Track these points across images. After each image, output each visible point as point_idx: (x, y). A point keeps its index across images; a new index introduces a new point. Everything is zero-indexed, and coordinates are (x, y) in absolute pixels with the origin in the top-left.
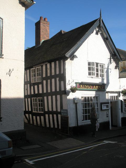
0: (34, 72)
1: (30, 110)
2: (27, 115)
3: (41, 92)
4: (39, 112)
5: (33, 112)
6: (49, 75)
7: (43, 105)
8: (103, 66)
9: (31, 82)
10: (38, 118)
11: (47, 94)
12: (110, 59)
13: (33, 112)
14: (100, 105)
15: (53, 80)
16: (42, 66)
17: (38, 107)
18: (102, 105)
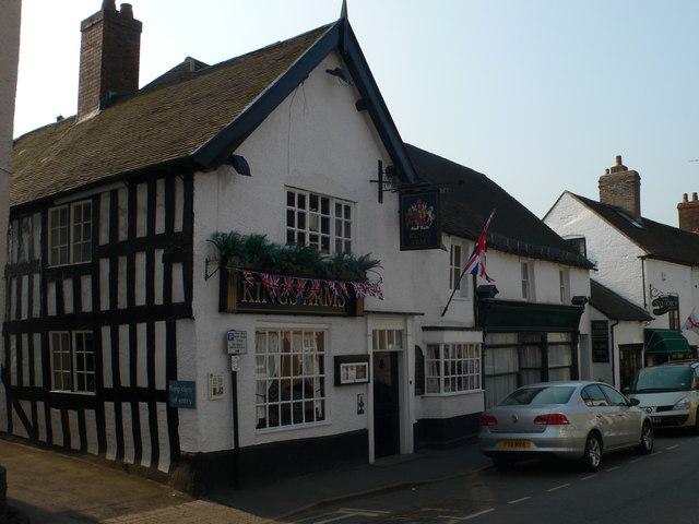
0: (63, 223)
1: (39, 382)
2: (26, 406)
3: (87, 306)
6: (123, 235)
7: (95, 361)
8: (348, 209)
9: (49, 262)
10: (73, 415)
11: (115, 318)
12: (380, 182)
14: (332, 364)
15: (141, 260)
16: (97, 198)
17: (76, 372)
18: (342, 365)
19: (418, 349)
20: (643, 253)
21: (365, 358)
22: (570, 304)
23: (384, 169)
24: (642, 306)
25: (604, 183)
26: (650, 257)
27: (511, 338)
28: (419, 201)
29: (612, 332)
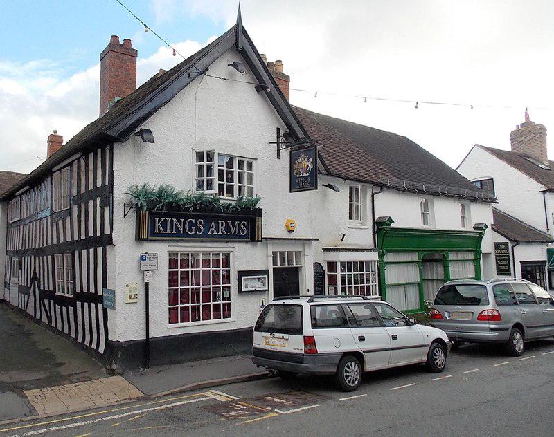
8: (250, 166)
12: (278, 143)
14: (236, 278)
18: (243, 278)
19: (317, 266)
20: (544, 188)
21: (266, 272)
22: (473, 230)
23: (282, 133)
24: (546, 231)
25: (515, 136)
26: (551, 191)
29: (513, 252)
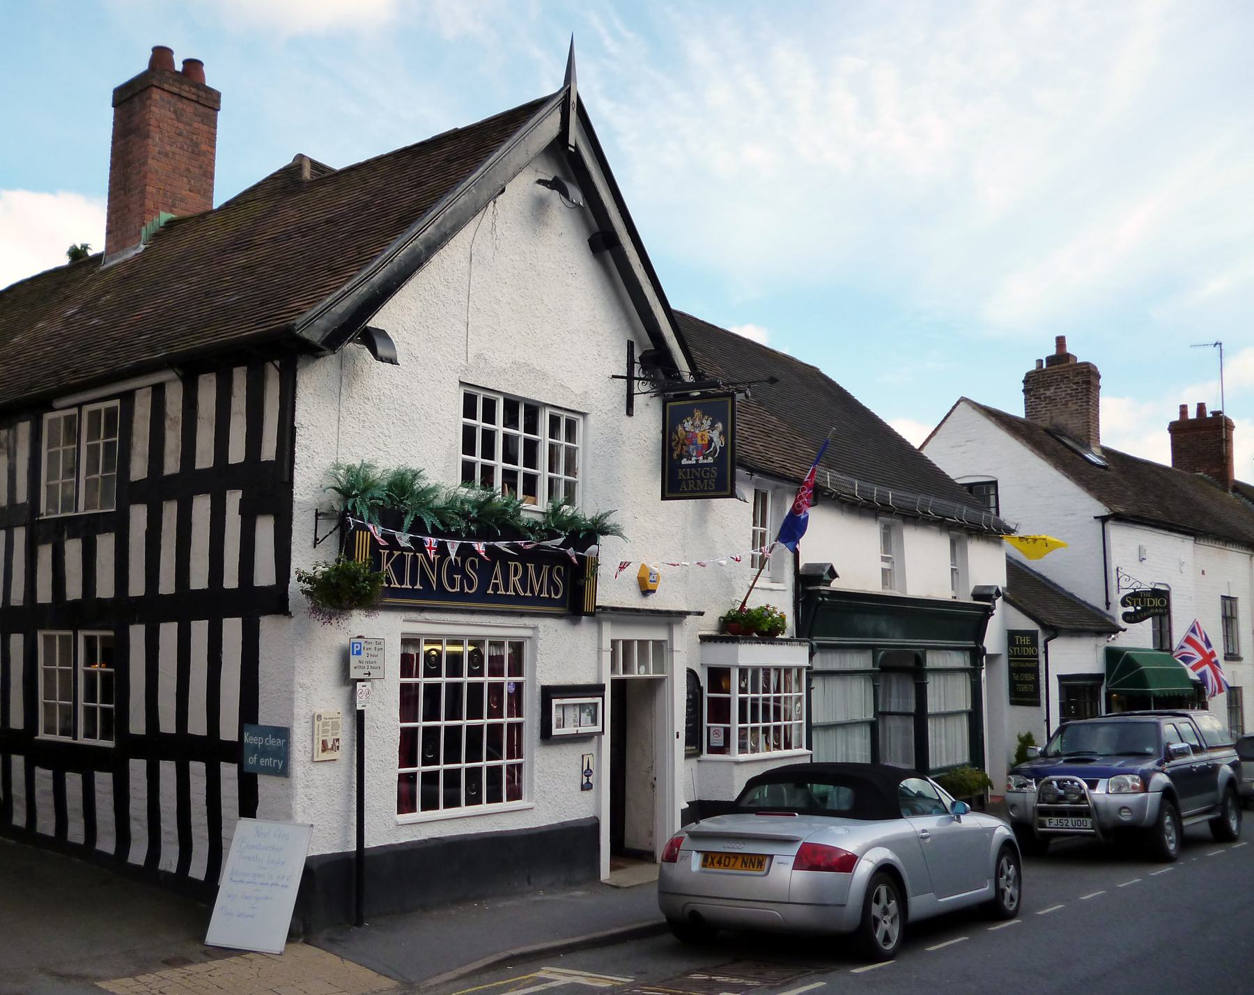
4: (82, 740)
5: (42, 735)
6: (172, 465)
7: (117, 687)
8: (571, 426)
9: (43, 508)
10: (74, 781)
12: (630, 378)
13: (42, 735)
15: (202, 507)
16: (128, 398)
18: (555, 702)
19: (692, 675)
20: (1103, 510)
21: (597, 690)
22: (969, 600)
23: (637, 354)
24: (1102, 607)
25: (1034, 383)
26: (1118, 518)
27: (861, 661)
28: (698, 414)
29: (1046, 653)
